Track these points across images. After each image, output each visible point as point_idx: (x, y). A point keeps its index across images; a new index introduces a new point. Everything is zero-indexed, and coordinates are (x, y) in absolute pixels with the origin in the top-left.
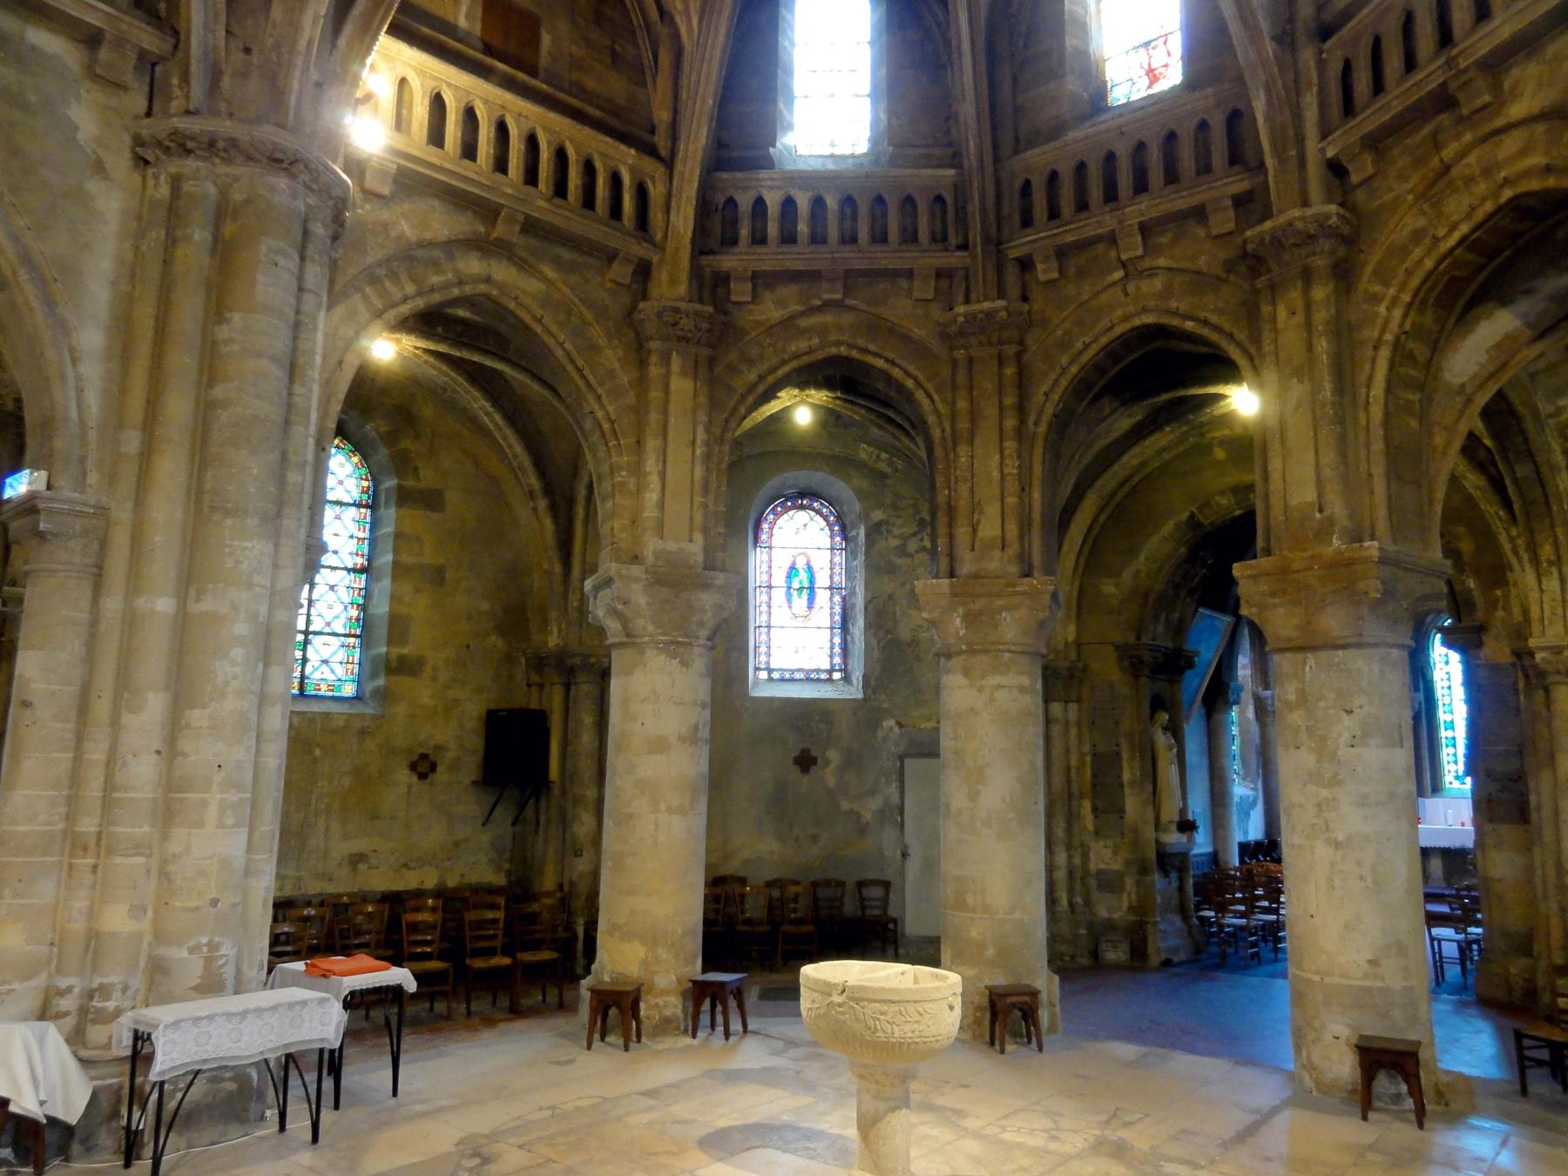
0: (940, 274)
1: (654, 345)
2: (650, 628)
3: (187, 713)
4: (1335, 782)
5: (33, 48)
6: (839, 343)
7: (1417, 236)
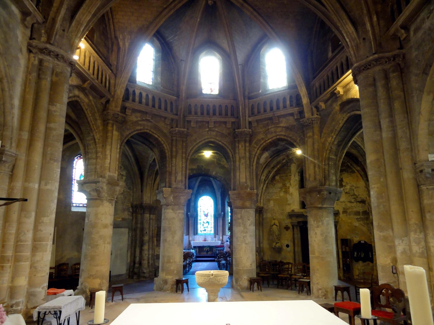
0: (172, 120)
1: (111, 122)
2: (106, 195)
3: (42, 218)
4: (246, 232)
5: (13, 11)
6: (147, 129)
7: (263, 139)
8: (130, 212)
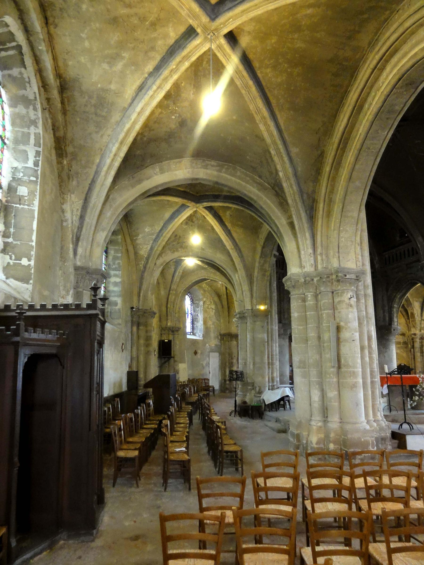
8: (218, 339)
